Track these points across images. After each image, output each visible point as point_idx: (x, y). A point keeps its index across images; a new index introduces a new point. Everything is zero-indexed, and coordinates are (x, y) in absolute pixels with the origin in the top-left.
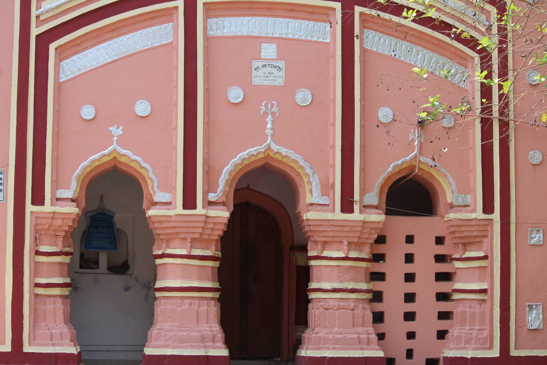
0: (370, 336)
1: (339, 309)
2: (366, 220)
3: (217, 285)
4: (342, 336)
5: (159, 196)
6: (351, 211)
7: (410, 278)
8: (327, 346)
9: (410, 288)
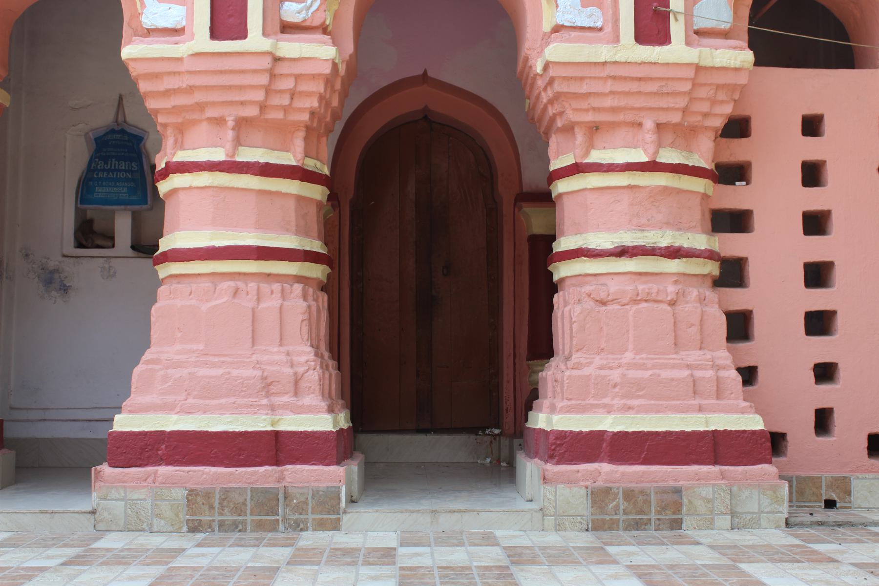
0: (723, 373)
1: (635, 301)
2: (702, 64)
4: (647, 374)
6: (664, 38)
7: (815, 223)
8: (606, 401)
9: (817, 249)
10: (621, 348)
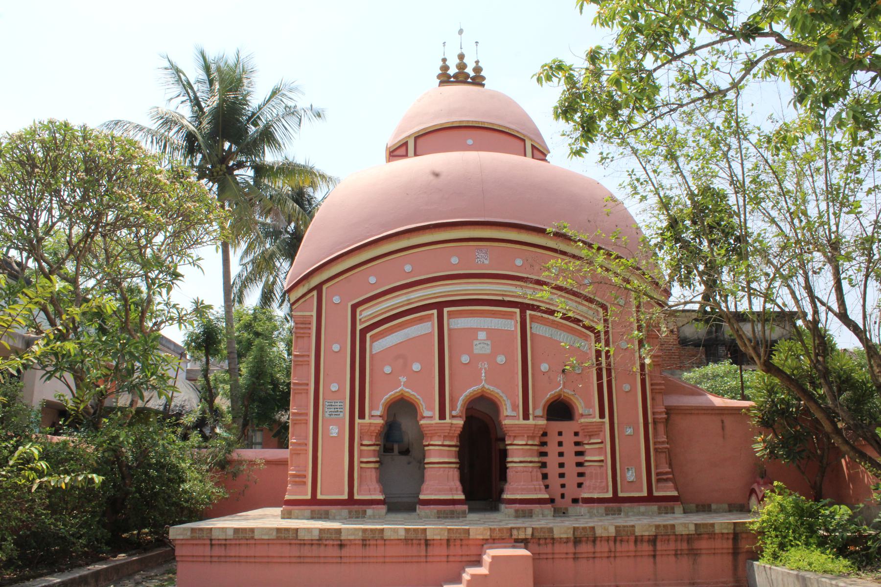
3: (457, 460)
5: (426, 413)
9: (561, 460)
10: (520, 483)
